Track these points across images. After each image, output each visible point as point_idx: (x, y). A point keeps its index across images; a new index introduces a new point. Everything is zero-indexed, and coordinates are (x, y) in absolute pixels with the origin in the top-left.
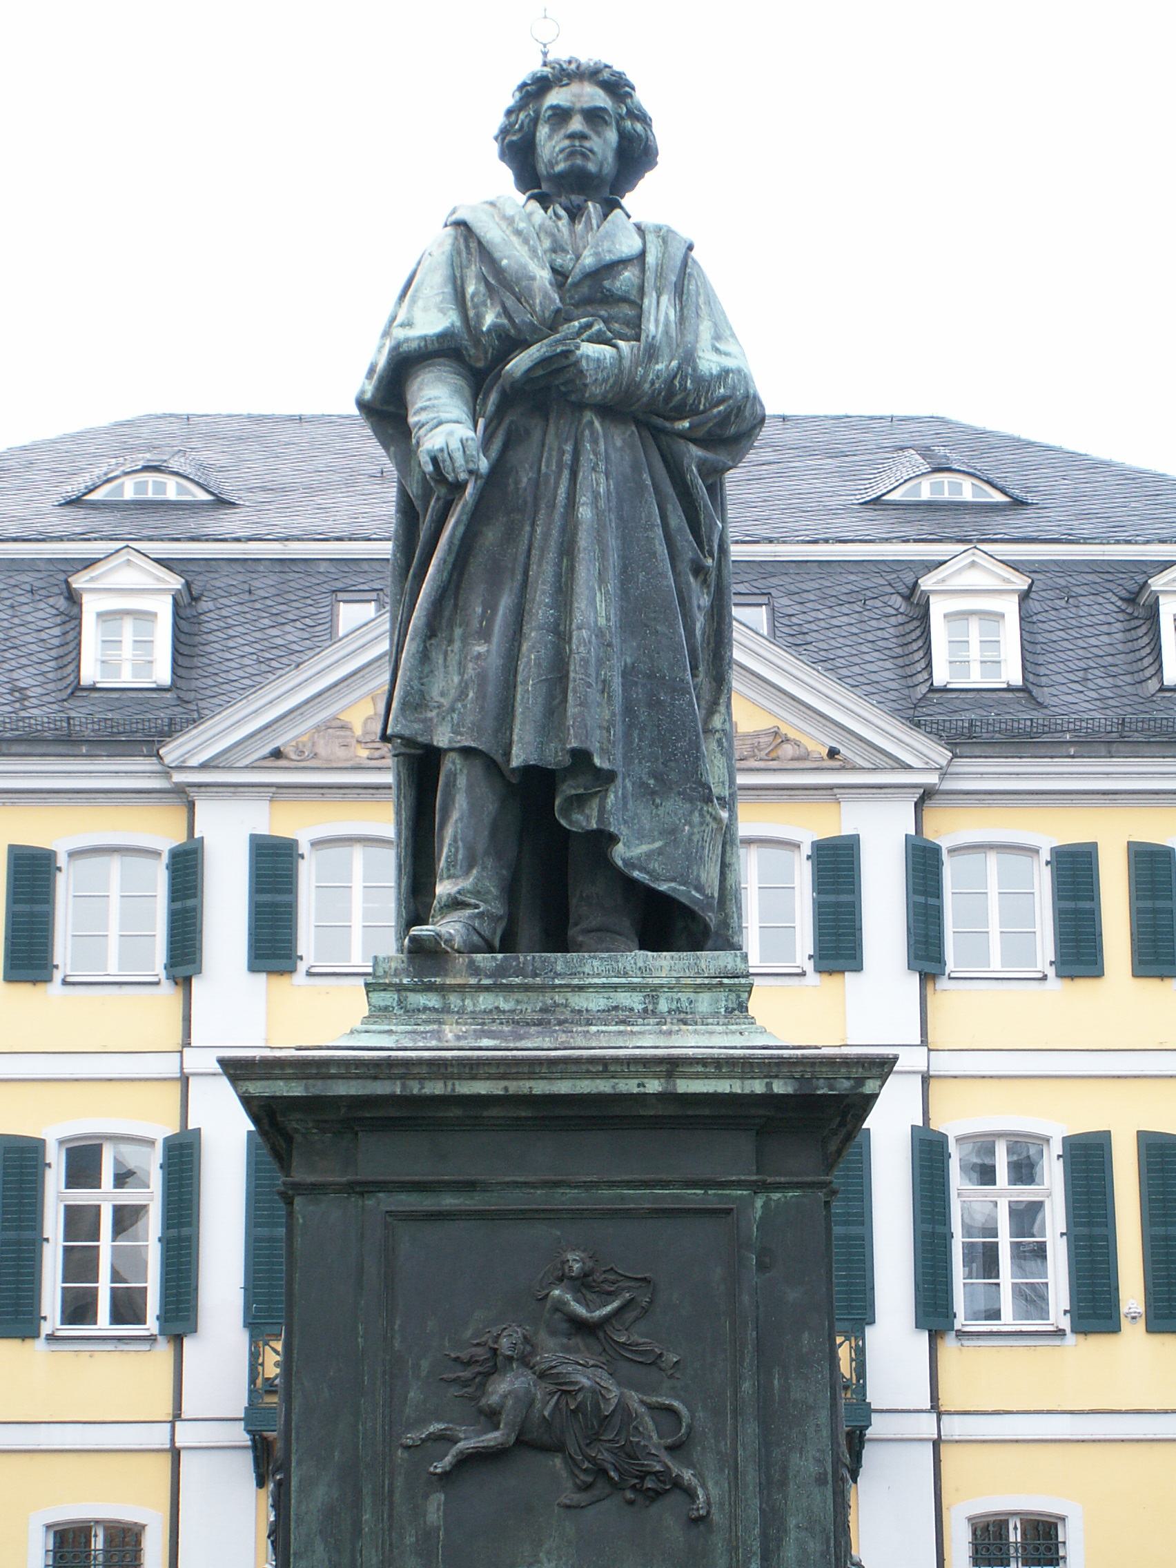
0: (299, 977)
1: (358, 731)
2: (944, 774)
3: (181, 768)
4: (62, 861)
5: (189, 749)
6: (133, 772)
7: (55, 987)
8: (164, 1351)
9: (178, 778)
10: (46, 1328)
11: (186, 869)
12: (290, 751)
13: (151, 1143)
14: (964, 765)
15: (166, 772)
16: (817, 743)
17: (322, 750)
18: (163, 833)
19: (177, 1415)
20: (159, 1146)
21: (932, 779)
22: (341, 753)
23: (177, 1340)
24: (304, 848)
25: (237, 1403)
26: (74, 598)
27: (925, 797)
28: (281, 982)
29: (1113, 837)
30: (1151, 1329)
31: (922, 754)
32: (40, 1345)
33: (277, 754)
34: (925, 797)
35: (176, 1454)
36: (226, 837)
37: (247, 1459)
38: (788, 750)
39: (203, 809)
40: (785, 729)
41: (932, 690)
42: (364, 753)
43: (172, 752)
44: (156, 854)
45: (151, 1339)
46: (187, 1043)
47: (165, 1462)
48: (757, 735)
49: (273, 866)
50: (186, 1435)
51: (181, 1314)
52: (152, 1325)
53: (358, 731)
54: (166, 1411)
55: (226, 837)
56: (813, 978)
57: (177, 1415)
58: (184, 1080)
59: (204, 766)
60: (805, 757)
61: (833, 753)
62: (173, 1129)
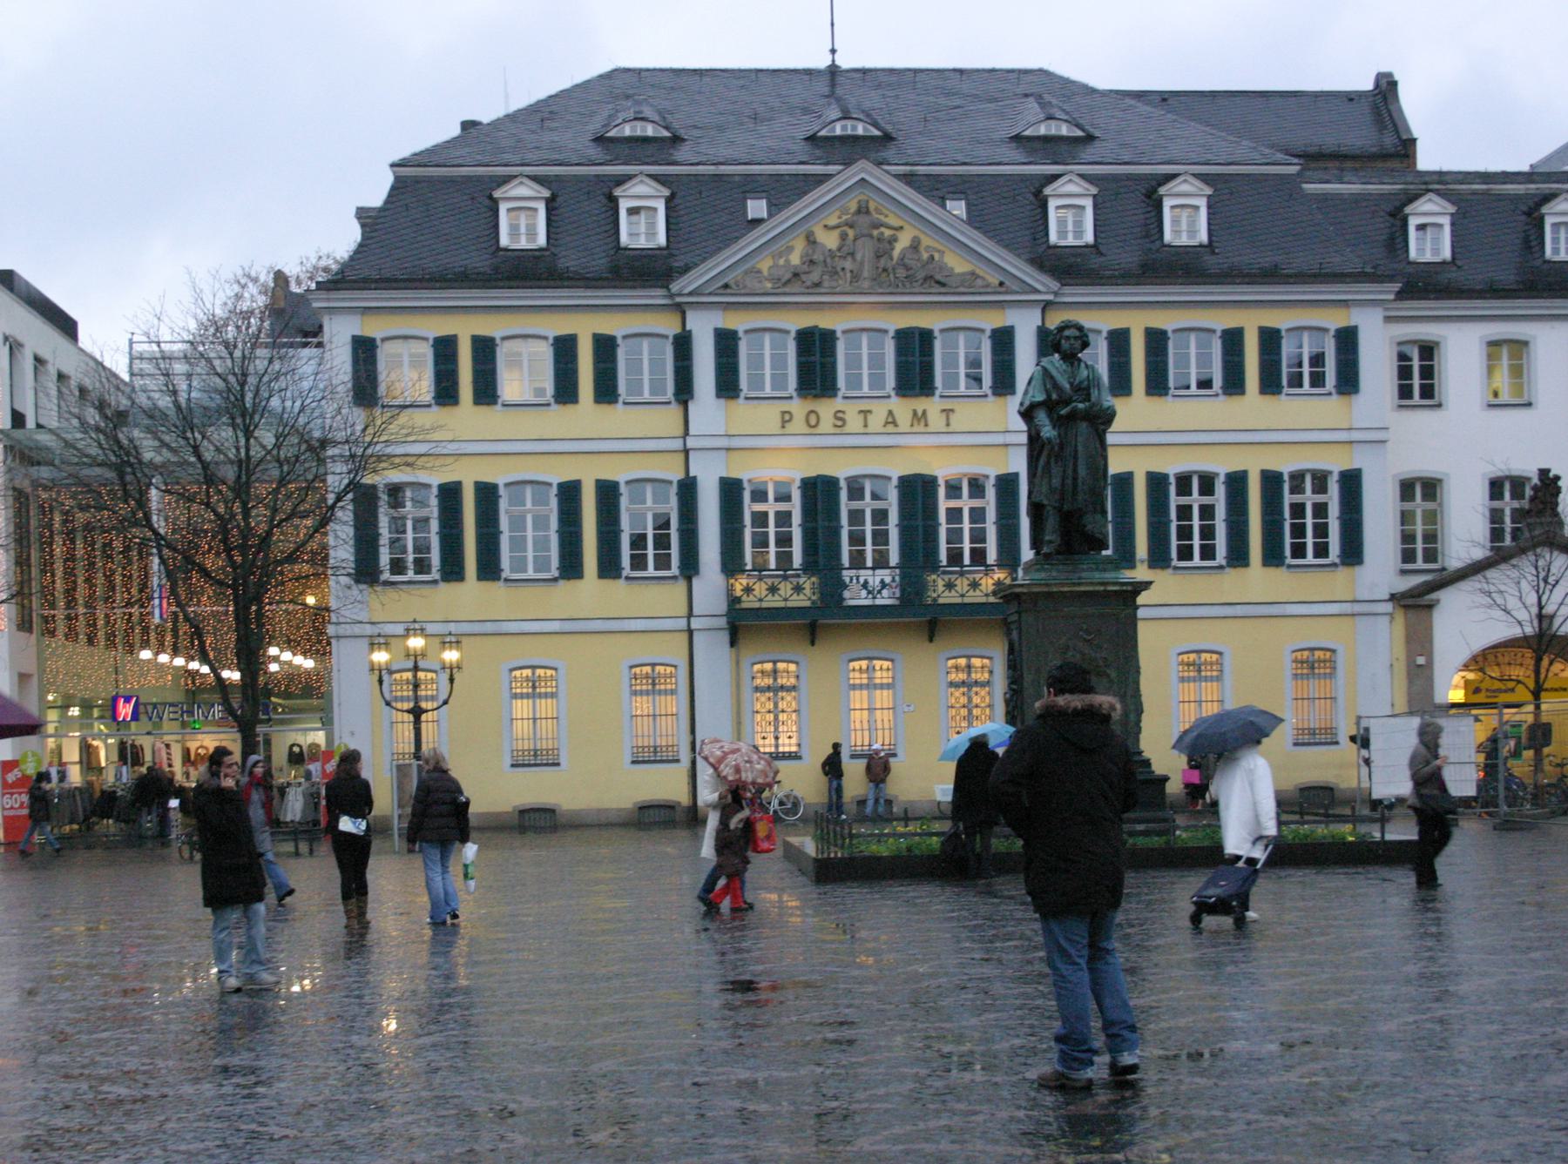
0: (741, 400)
1: (765, 273)
2: (1056, 294)
3: (680, 295)
4: (619, 341)
5: (681, 285)
6: (656, 296)
7: (620, 406)
8: (681, 586)
9: (678, 299)
10: (624, 573)
11: (683, 345)
12: (732, 284)
13: (670, 482)
14: (1067, 290)
15: (672, 296)
16: (994, 279)
17: (749, 284)
18: (668, 326)
19: (690, 615)
20: (675, 485)
21: (1050, 297)
22: (758, 285)
23: (689, 579)
24: (741, 334)
25: (721, 606)
26: (613, 202)
27: (1046, 306)
28: (732, 403)
29: (1137, 324)
30: (1150, 567)
31: (1045, 285)
32: (621, 582)
33: (726, 286)
34: (1046, 306)
35: (690, 632)
36: (703, 330)
37: (725, 637)
38: (979, 282)
39: (690, 315)
40: (978, 271)
41: (1050, 247)
42: (769, 285)
43: (675, 287)
44: (666, 337)
45: (674, 578)
46: (686, 432)
47: (685, 636)
48: (964, 274)
49: (726, 343)
50: (696, 624)
51: (690, 566)
52: (675, 569)
53: (765, 273)
54: (684, 611)
55: (703, 330)
56: (991, 398)
57: (690, 615)
58: (686, 452)
59: (690, 294)
60: (987, 286)
61: (1001, 284)
62: (681, 476)
